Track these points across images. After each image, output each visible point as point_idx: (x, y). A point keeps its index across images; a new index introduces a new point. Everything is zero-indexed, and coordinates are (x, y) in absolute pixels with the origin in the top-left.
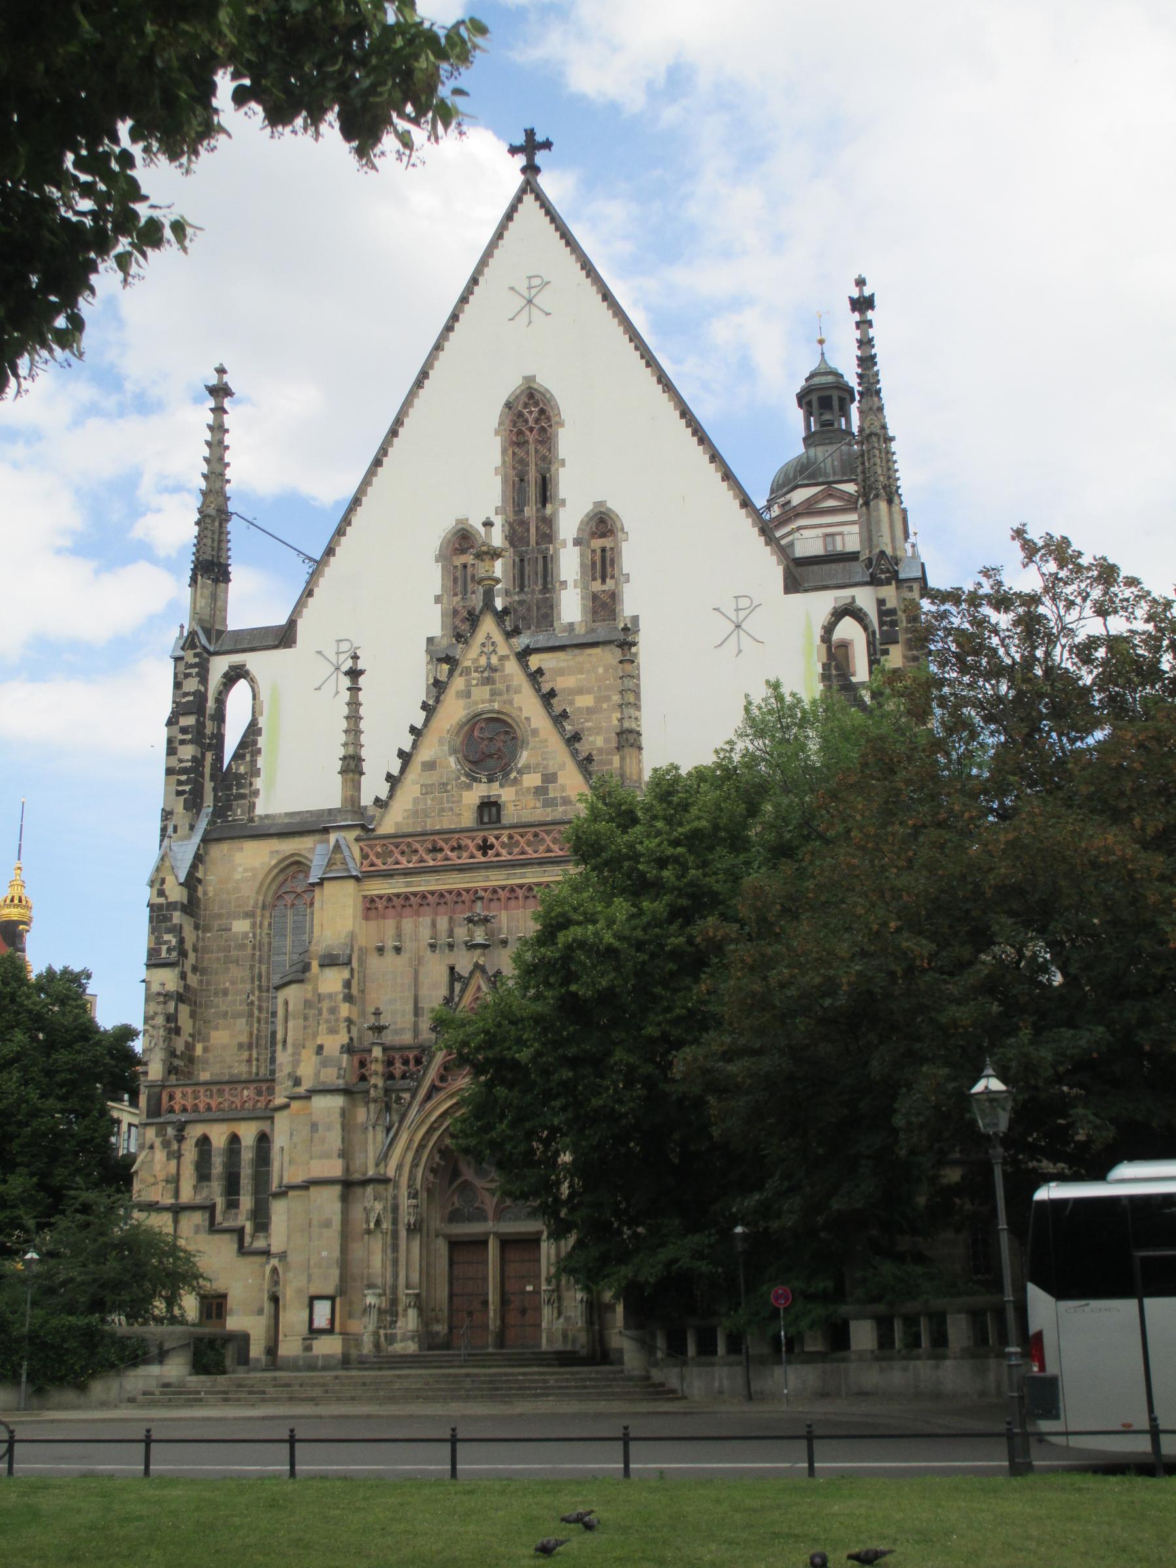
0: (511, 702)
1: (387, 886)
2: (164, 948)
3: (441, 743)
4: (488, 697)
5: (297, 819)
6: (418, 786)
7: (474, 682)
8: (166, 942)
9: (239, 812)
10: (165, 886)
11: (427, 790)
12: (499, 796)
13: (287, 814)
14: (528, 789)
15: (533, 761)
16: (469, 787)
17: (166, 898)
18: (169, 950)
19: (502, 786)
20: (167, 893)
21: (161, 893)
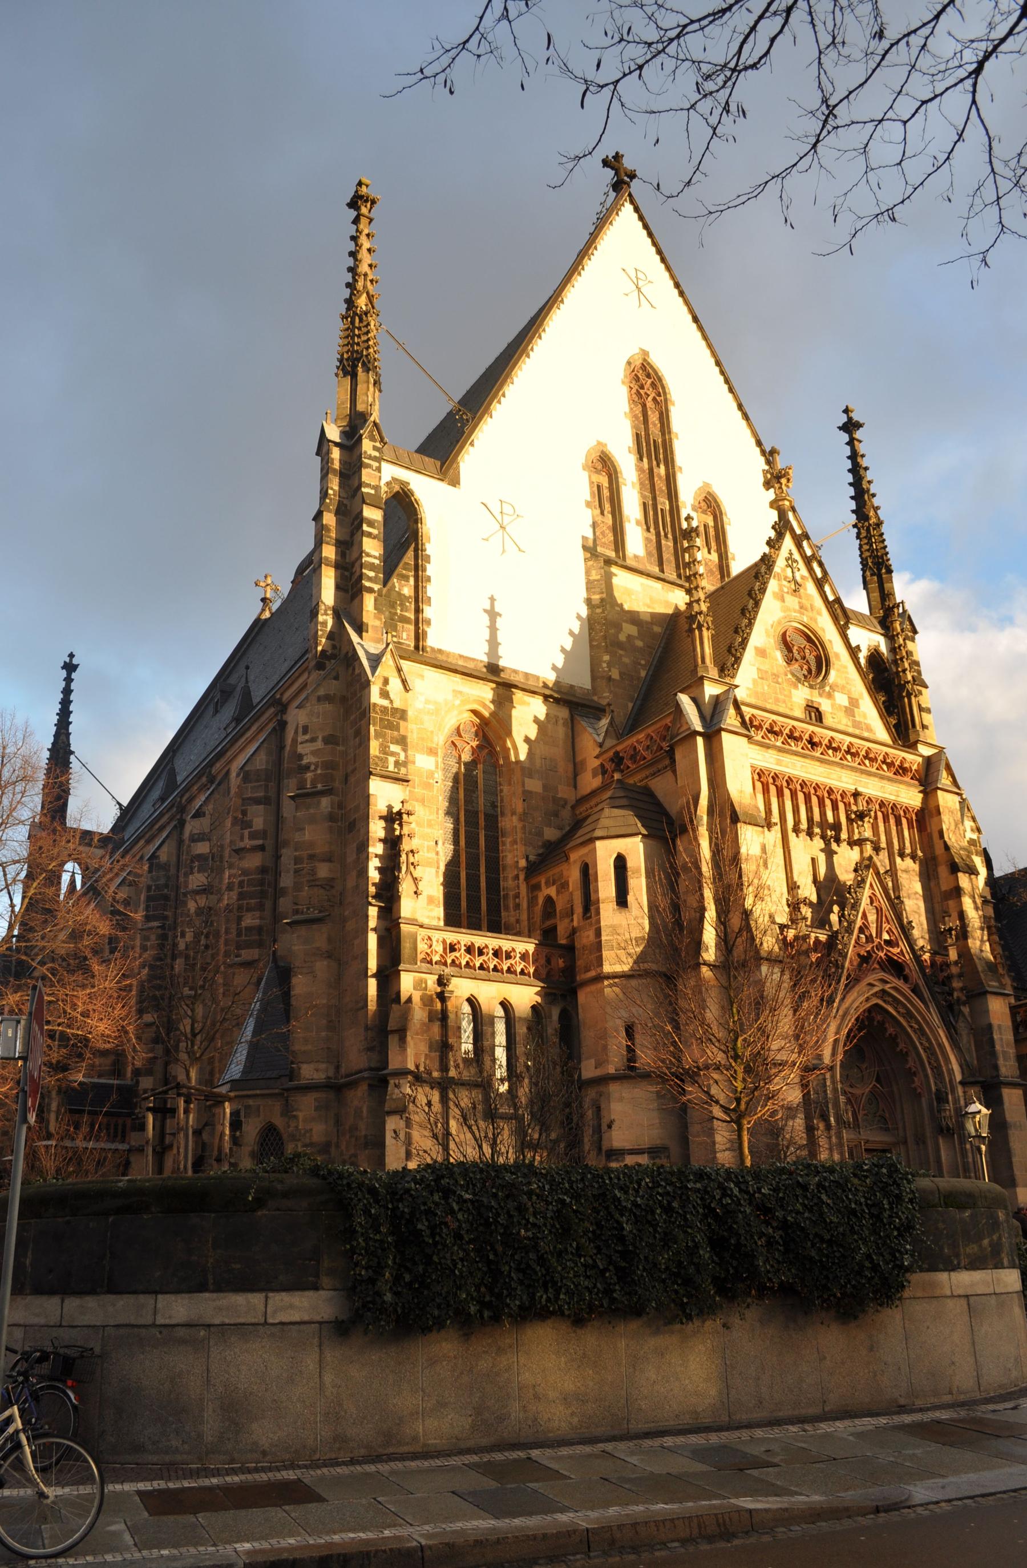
0: (815, 621)
1: (760, 757)
2: (391, 760)
3: (768, 635)
4: (797, 607)
5: (471, 665)
6: (755, 669)
7: (786, 590)
8: (393, 754)
9: (405, 636)
10: (388, 688)
11: (763, 675)
12: (820, 704)
13: (461, 656)
14: (840, 706)
15: (841, 682)
16: (796, 687)
17: (391, 702)
18: (397, 763)
19: (820, 695)
20: (392, 696)
21: (385, 694)
